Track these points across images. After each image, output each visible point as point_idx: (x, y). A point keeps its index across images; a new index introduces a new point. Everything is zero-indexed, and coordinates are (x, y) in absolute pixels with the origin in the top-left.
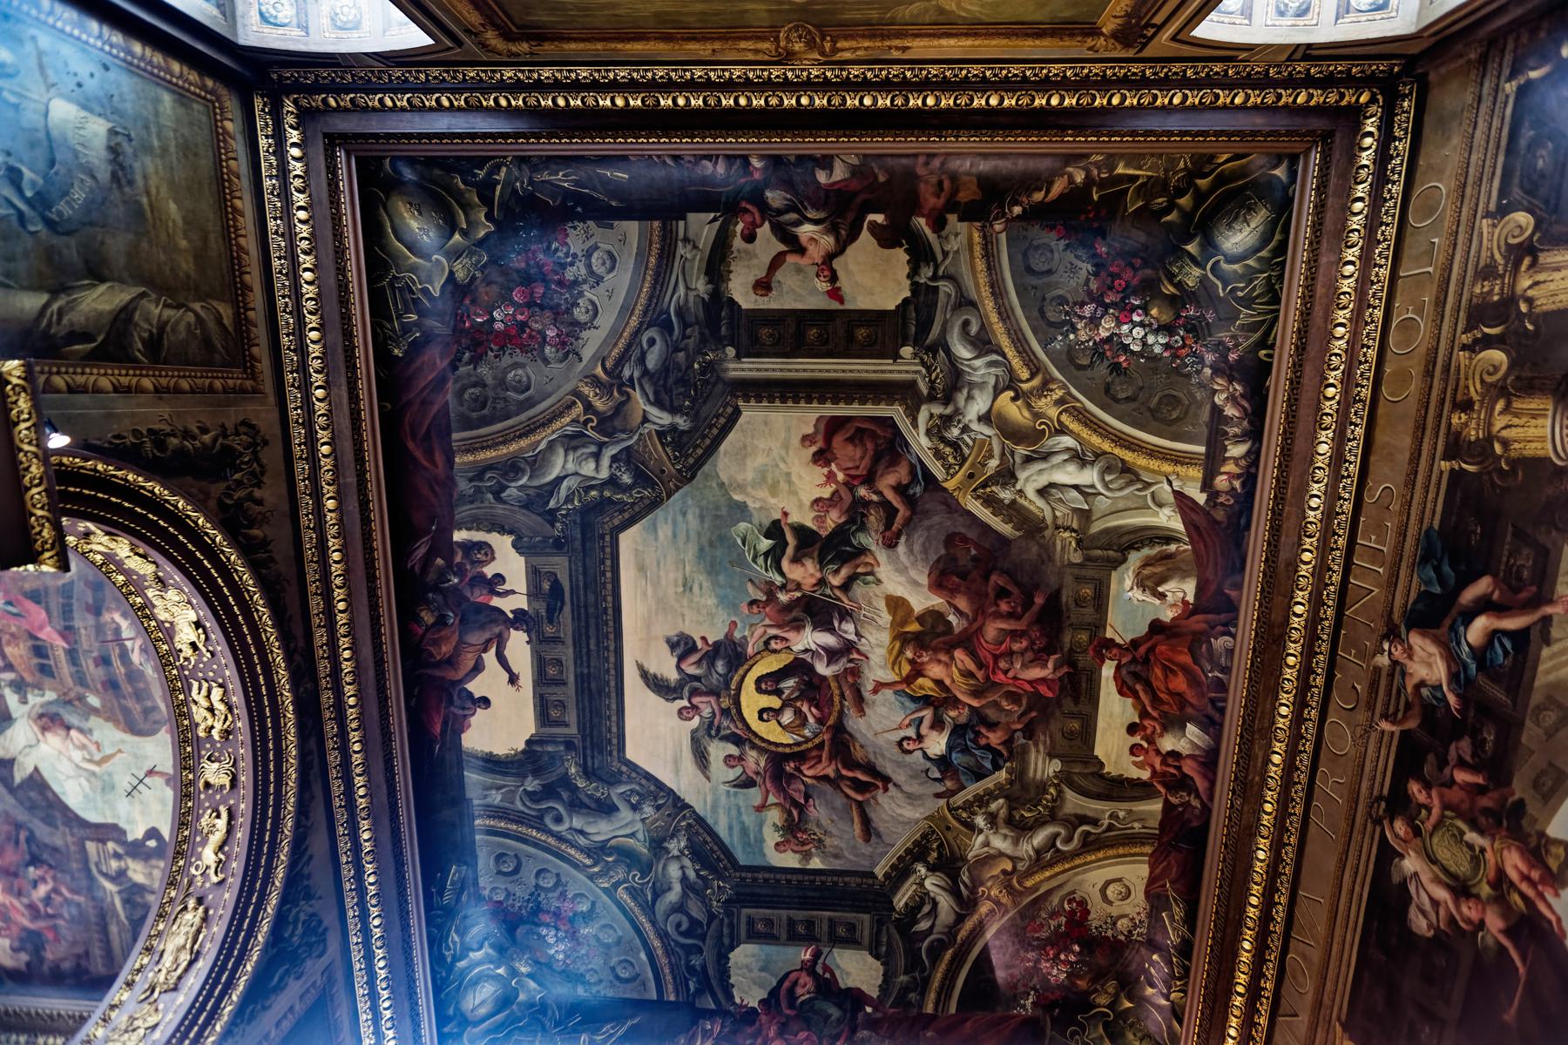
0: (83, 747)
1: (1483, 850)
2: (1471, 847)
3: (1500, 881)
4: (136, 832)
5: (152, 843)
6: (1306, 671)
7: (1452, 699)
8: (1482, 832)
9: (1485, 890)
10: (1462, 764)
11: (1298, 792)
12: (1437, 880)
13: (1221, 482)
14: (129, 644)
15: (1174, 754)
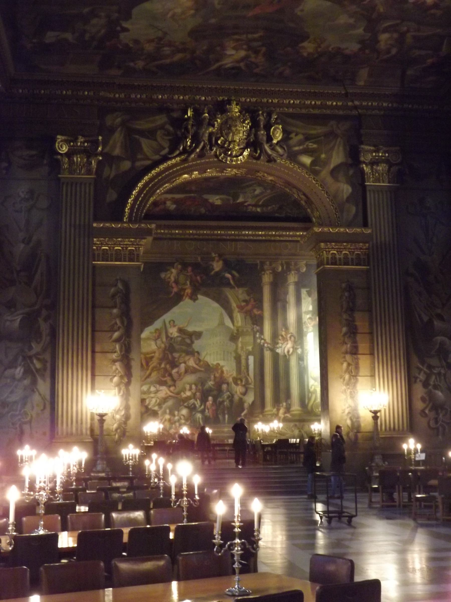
0: (183, 13)
1: (187, 285)
2: (186, 282)
3: (185, 289)
4: (126, 25)
5: (119, 28)
6: (204, 234)
7: (212, 273)
8: (190, 284)
9: (180, 287)
10: (201, 278)
11: (168, 236)
12: (175, 277)
13: (251, 207)
14: (245, 36)
15: (165, 203)
